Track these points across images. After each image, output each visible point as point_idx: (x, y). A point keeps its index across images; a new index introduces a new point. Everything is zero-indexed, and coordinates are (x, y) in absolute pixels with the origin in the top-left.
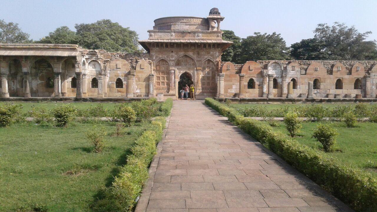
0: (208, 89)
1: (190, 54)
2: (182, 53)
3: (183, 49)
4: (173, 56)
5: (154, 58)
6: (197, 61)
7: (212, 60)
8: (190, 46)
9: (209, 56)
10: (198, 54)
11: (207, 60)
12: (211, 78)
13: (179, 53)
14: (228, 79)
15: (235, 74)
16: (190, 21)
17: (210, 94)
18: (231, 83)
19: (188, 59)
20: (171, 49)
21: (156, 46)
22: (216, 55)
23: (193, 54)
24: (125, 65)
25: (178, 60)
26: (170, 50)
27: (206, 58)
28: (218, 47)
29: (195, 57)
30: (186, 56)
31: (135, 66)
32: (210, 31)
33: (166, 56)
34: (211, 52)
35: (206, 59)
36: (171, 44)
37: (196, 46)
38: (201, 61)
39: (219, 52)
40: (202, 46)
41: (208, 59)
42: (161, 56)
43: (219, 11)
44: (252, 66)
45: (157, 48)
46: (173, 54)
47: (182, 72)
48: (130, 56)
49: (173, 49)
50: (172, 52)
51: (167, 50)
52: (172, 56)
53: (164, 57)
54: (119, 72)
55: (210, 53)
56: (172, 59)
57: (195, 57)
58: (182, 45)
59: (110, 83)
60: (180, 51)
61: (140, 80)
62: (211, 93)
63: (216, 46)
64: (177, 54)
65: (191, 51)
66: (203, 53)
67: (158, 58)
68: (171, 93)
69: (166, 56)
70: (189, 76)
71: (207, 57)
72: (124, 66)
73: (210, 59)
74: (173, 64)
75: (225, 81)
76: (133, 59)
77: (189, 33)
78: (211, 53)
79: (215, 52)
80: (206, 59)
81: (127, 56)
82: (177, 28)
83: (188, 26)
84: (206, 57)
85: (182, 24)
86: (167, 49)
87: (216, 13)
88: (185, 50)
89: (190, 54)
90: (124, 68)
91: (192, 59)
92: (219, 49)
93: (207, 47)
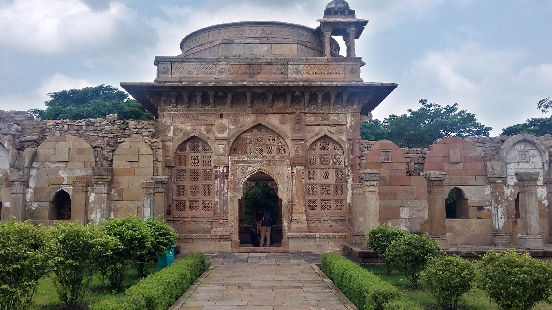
0: (325, 220)
1: (274, 121)
2: (248, 121)
3: (251, 107)
4: (220, 128)
5: (170, 134)
6: (293, 140)
7: (336, 138)
8: (270, 97)
9: (325, 127)
10: (298, 120)
11: (320, 136)
12: (332, 189)
13: (241, 118)
14: (388, 188)
15: (405, 174)
16: (271, 34)
17: (331, 235)
18: (397, 202)
19: (265, 134)
20: (217, 108)
21: (174, 101)
22: (347, 123)
23: (283, 122)
24: (80, 152)
25: (238, 138)
26: (216, 110)
27: (317, 131)
28: (350, 102)
29: (287, 129)
30: (259, 126)
31: (111, 154)
32: (326, 58)
33: (203, 129)
34: (330, 115)
35: (317, 135)
36: (216, 93)
37: (289, 97)
38: (302, 140)
39: (353, 116)
40: (307, 97)
41: (323, 134)
42: (189, 128)
43: (351, 8)
44: (455, 152)
45: (179, 106)
46: (224, 121)
47: (252, 169)
48: (99, 128)
49: (226, 109)
50: (221, 115)
51: (208, 110)
52: (222, 129)
53: (200, 130)
54: (61, 173)
55: (328, 119)
56: (219, 136)
57: (287, 129)
58: (249, 96)
59: (35, 205)
60: (242, 114)
61: (124, 195)
62: (335, 232)
63: (345, 99)
64: (236, 122)
65: (273, 114)
66: (309, 118)
67: (181, 135)
68: (218, 234)
69: (203, 129)
70: (274, 187)
71: (320, 130)
72: (77, 157)
73: (328, 134)
74: (224, 150)
75: (382, 195)
76: (106, 135)
77: (270, 64)
78: (333, 117)
79: (342, 116)
80: (317, 135)
81: (90, 128)
82: (235, 53)
83: (265, 48)
84: (317, 128)
85: (248, 41)
86: (207, 108)
87: (343, 13)
88: (257, 110)
89: (274, 121)
90: (78, 161)
91: (279, 136)
92: (355, 107)
93: (320, 101)
